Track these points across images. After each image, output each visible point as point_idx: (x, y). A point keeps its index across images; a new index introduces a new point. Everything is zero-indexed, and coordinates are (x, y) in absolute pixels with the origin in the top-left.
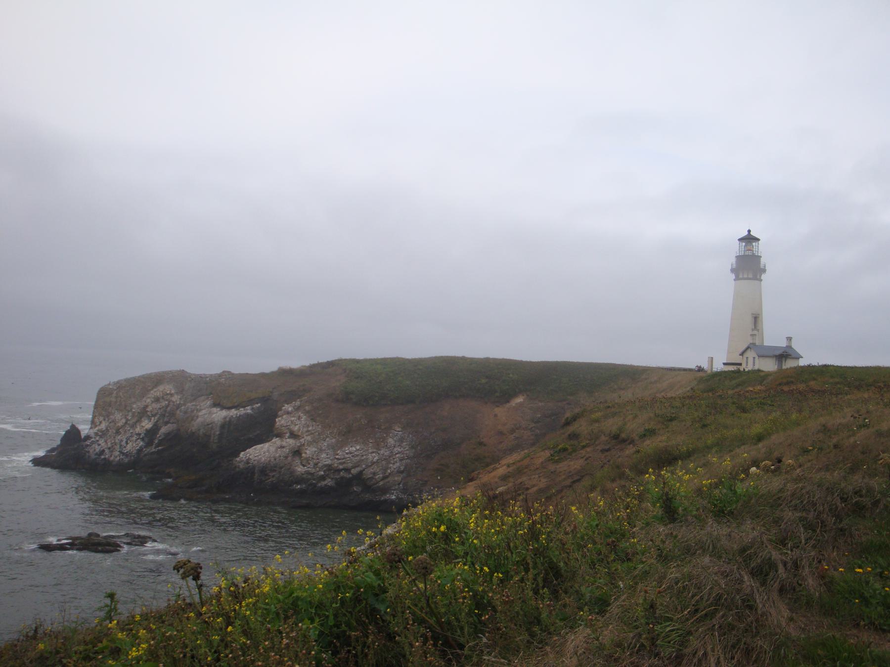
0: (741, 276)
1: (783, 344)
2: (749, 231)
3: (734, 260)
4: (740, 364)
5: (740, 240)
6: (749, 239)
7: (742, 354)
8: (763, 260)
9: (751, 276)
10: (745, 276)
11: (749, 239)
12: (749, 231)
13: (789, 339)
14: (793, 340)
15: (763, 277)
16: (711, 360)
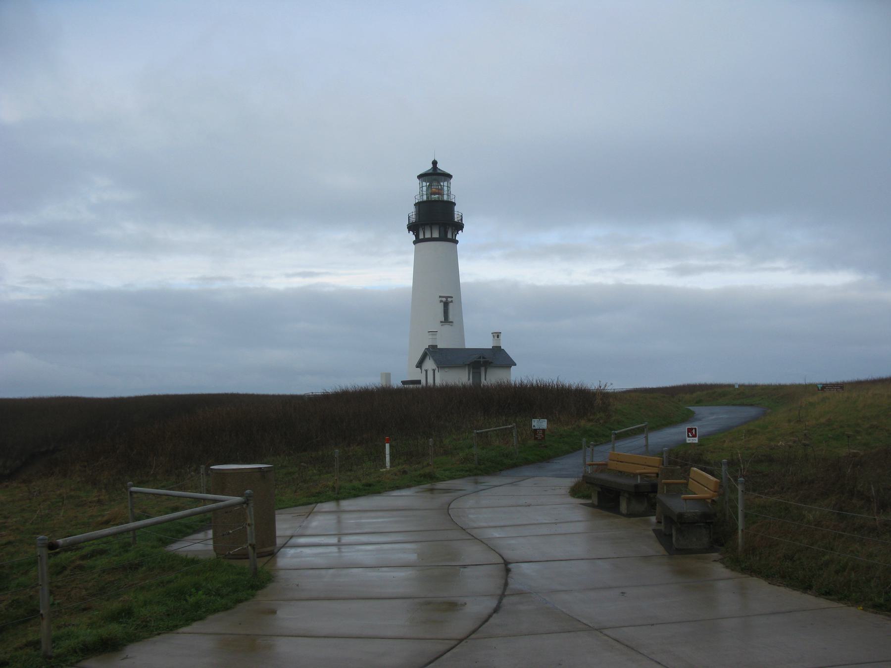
0: (421, 237)
1: (487, 343)
2: (435, 163)
3: (412, 210)
4: (419, 382)
5: (420, 177)
6: (435, 176)
7: (420, 365)
8: (456, 208)
9: (436, 235)
10: (428, 236)
11: (435, 176)
12: (435, 163)
13: (497, 335)
14: (501, 337)
15: (460, 236)
16: (388, 376)
